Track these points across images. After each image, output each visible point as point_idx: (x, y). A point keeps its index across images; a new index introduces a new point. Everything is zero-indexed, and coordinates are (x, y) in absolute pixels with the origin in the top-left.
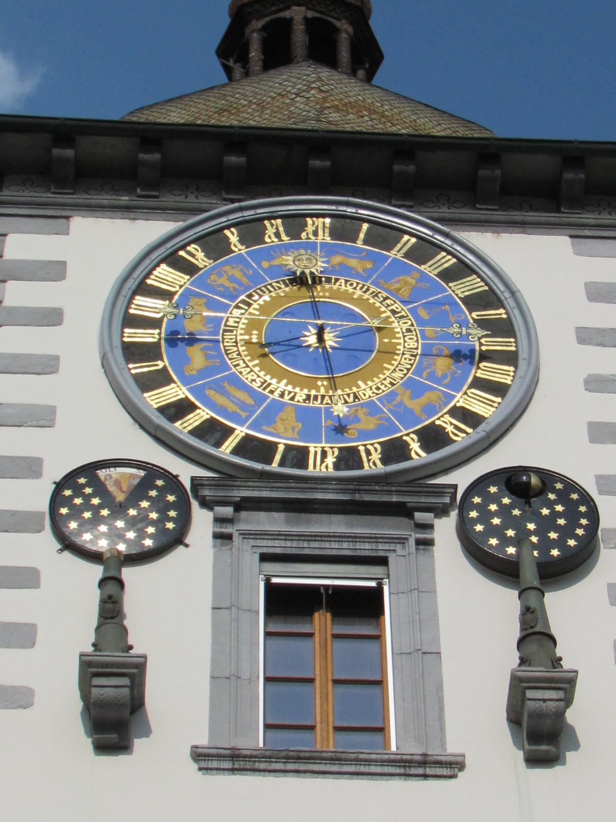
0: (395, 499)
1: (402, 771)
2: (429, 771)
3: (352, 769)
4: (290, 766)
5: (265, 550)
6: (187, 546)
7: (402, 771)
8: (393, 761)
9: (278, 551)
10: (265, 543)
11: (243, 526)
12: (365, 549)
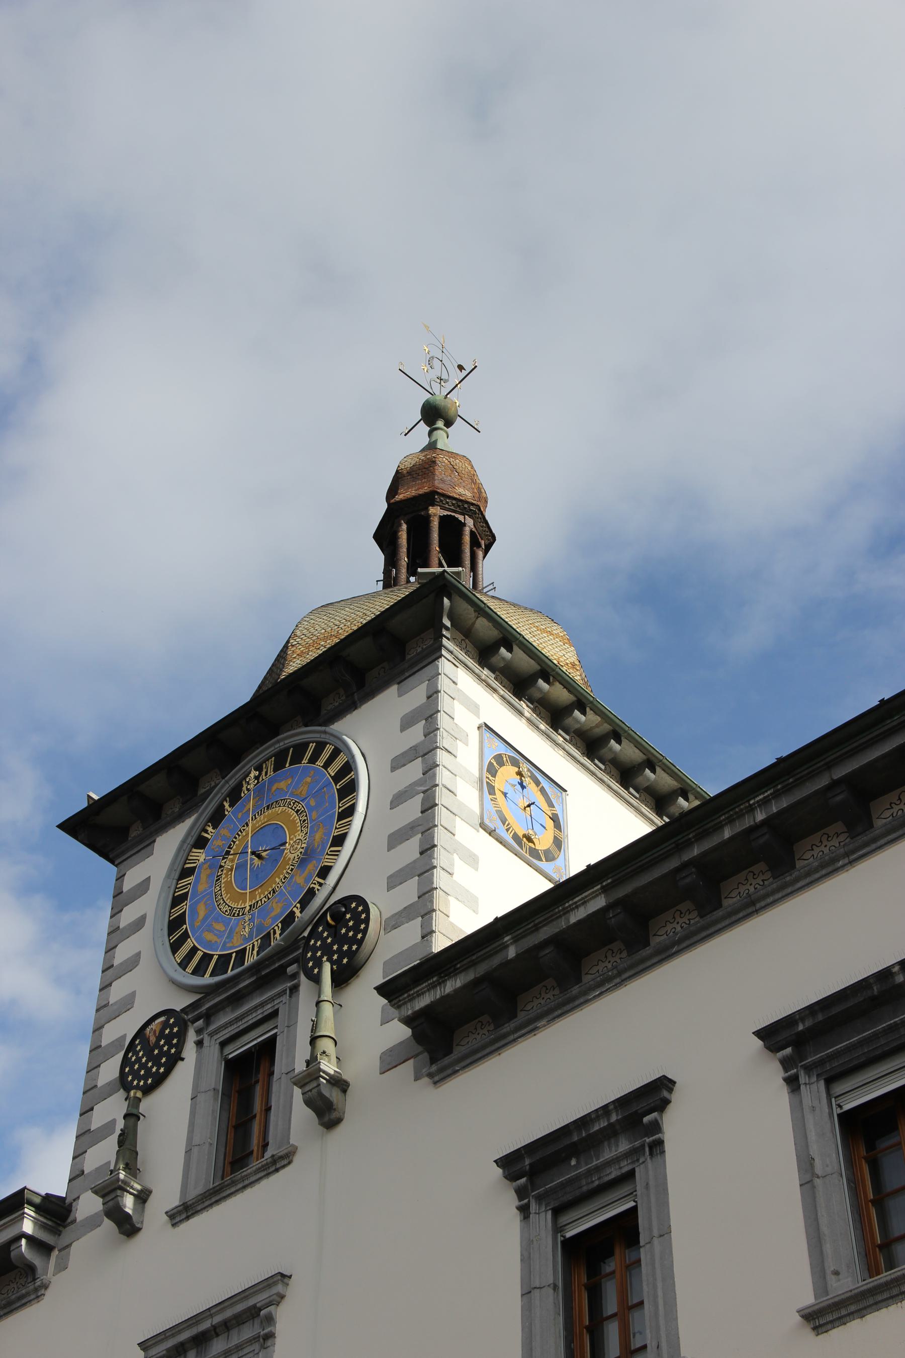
0: (277, 965)
1: (265, 1173)
2: (278, 1166)
3: (240, 1186)
4: (213, 1200)
5: (222, 1039)
6: (183, 1059)
7: (265, 1173)
8: (259, 1168)
9: (227, 1036)
10: (221, 1034)
11: (212, 1027)
12: (268, 1009)
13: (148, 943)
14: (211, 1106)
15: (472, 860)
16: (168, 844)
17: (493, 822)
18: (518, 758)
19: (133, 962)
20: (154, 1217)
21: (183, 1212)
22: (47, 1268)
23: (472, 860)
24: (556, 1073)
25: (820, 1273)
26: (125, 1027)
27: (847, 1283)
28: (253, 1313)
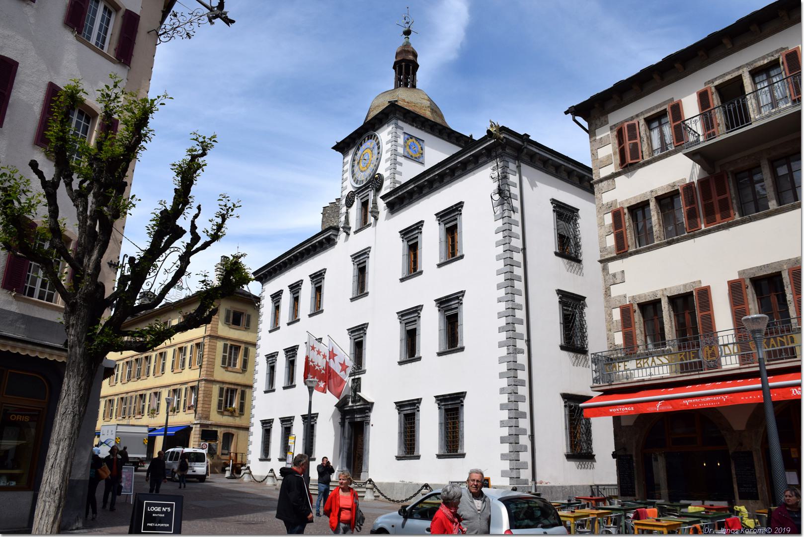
13: (348, 175)
14: (359, 211)
15: (401, 164)
16: (352, 152)
17: (406, 154)
18: (412, 137)
19: (346, 179)
20: (352, 232)
21: (356, 232)
22: (337, 240)
23: (401, 164)
24: (408, 217)
25: (441, 258)
26: (346, 193)
27: (443, 261)
28: (365, 253)
